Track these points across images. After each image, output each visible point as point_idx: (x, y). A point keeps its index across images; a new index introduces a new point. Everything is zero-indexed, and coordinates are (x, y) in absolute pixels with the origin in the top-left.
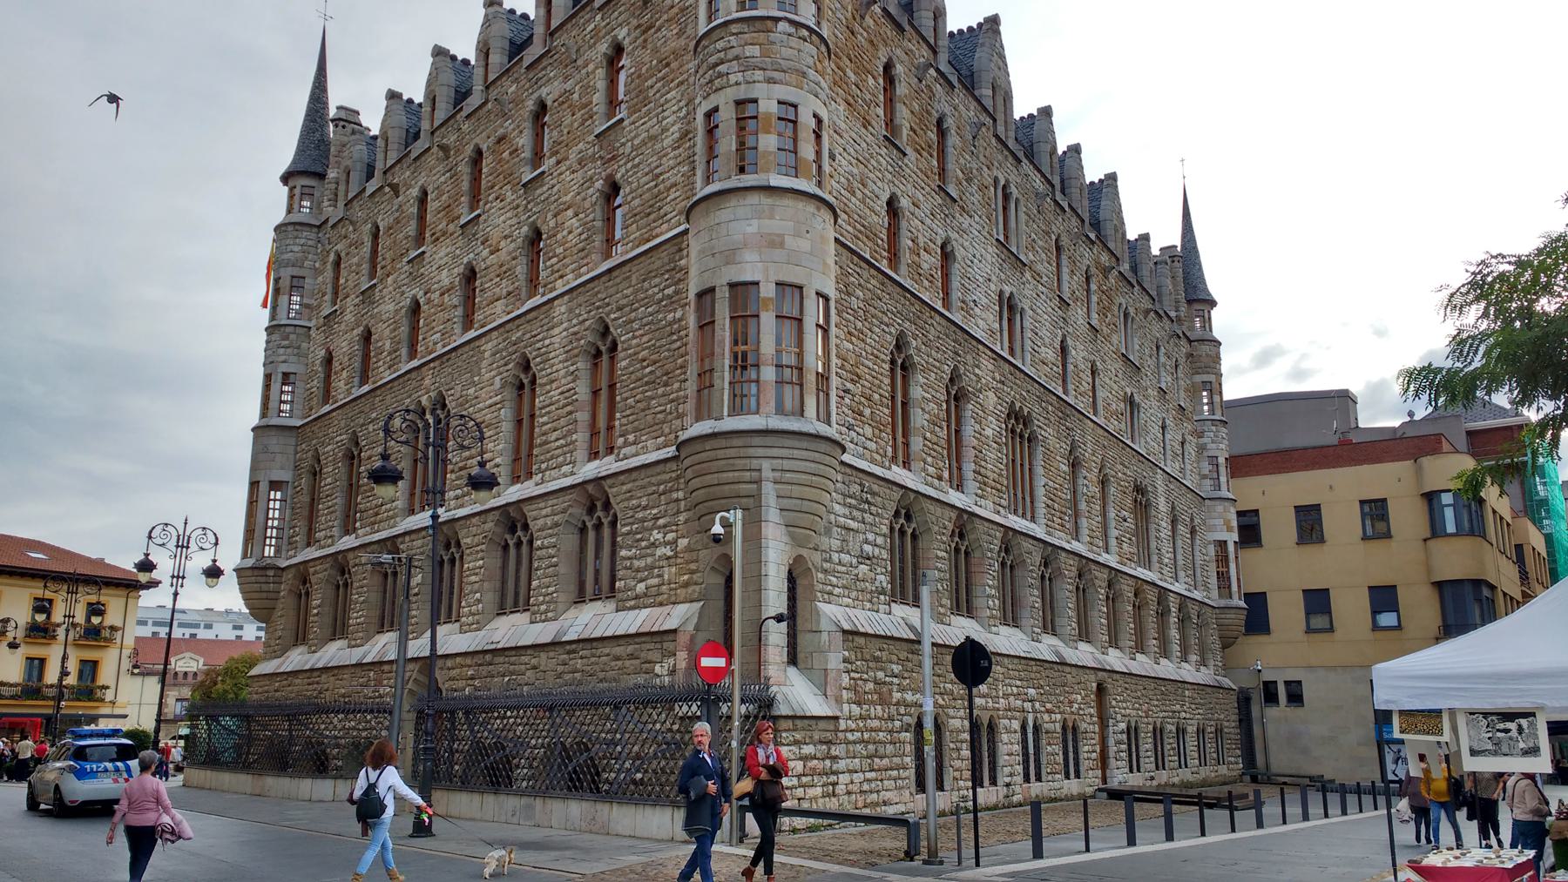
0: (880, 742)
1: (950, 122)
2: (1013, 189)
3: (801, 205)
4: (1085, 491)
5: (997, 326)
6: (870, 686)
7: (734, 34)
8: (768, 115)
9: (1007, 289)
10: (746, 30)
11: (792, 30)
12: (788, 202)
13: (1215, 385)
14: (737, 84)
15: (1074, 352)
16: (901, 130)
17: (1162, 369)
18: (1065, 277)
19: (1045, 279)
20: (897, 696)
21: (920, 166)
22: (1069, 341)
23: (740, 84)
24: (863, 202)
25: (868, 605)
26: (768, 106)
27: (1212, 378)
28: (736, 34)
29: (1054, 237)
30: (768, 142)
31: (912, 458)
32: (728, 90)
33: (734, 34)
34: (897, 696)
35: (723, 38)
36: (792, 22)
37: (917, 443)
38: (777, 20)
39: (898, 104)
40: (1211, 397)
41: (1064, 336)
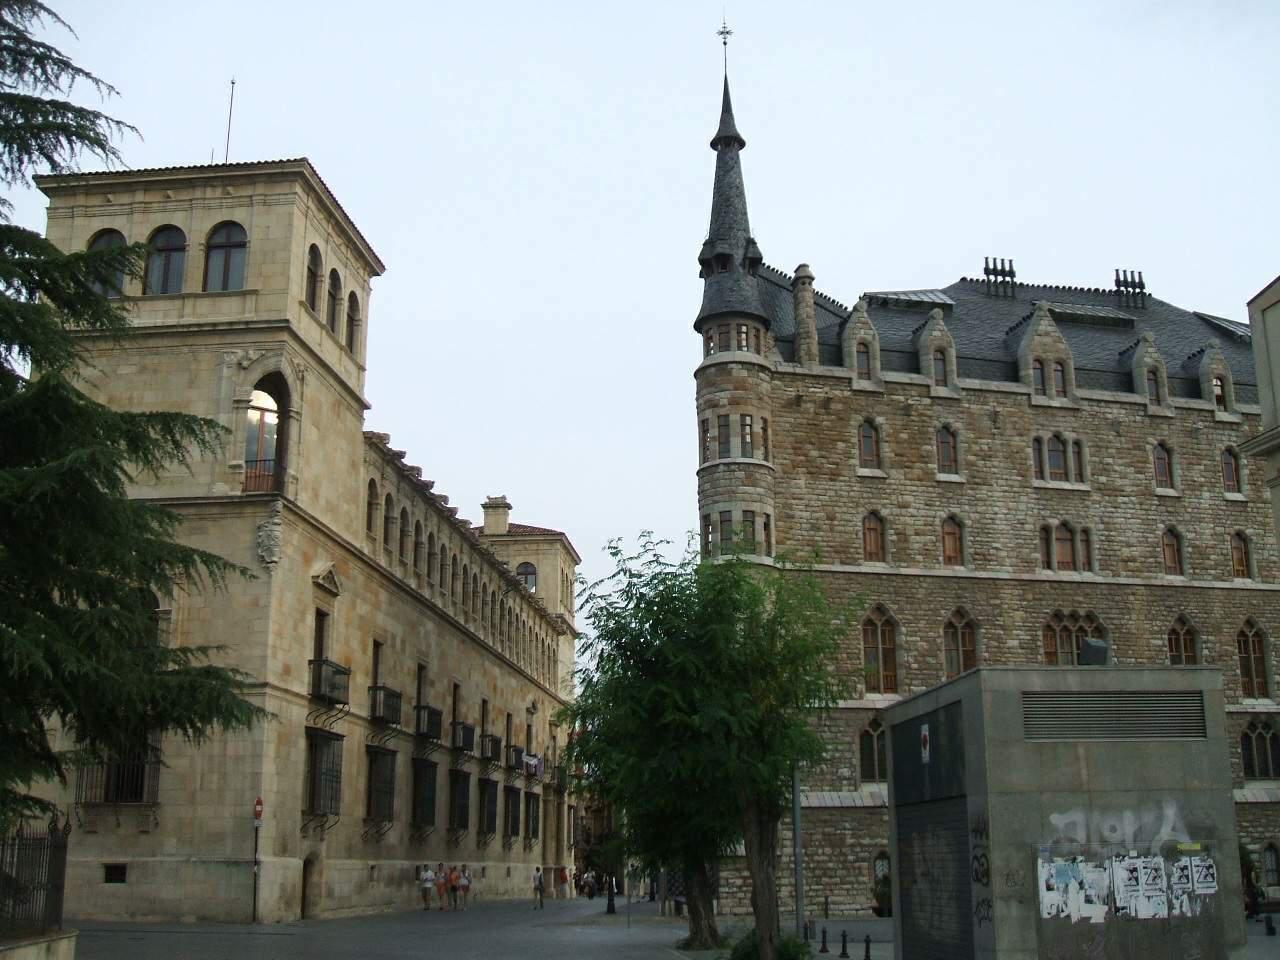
0: (829, 869)
1: (957, 425)
2: (1069, 436)
4: (1206, 652)
6: (819, 837)
9: (1054, 522)
11: (726, 468)
18: (1178, 472)
19: (1129, 489)
20: (850, 841)
21: (909, 476)
22: (1181, 528)
24: (832, 530)
25: (827, 788)
31: (899, 682)
34: (850, 841)
36: (724, 464)
37: (902, 673)
38: (718, 465)
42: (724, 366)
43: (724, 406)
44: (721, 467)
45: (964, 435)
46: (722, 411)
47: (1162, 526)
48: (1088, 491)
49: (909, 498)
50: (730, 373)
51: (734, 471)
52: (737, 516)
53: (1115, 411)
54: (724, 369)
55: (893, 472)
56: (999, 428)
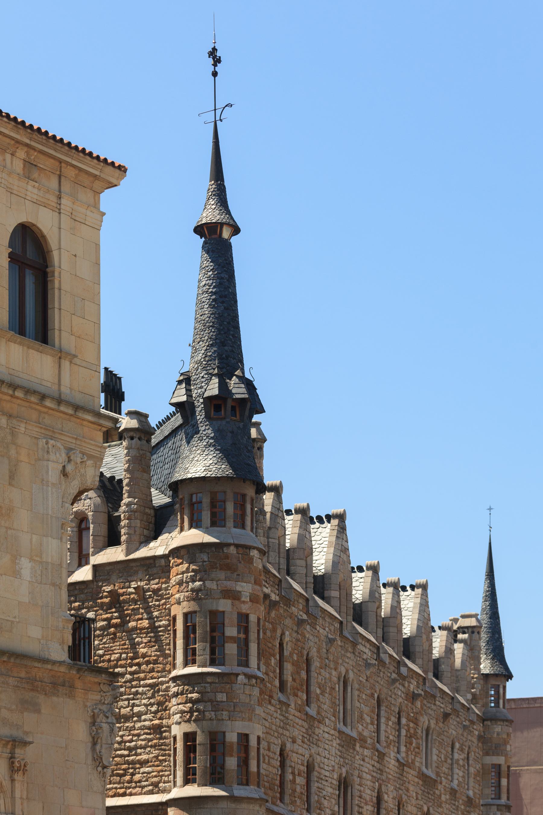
3: (251, 807)
5: (336, 808)
7: (208, 683)
8: (232, 743)
10: (217, 681)
12: (244, 806)
13: (504, 768)
14: (210, 719)
15: (386, 797)
16: (287, 684)
17: (455, 766)
18: (383, 727)
23: (213, 720)
26: (232, 737)
27: (500, 760)
28: (210, 683)
29: (376, 695)
30: (231, 763)
32: (204, 722)
33: (208, 683)
35: (200, 683)
36: (245, 675)
38: (237, 675)
39: (285, 663)
40: (497, 693)
41: (380, 786)
42: (248, 550)
43: (244, 602)
44: (241, 678)
45: (316, 664)
46: (245, 608)
47: (377, 783)
48: (355, 740)
49: (296, 733)
50: (250, 560)
51: (253, 686)
52: (253, 742)
53: (367, 651)
54: (248, 555)
55: (292, 698)
56: (327, 659)
